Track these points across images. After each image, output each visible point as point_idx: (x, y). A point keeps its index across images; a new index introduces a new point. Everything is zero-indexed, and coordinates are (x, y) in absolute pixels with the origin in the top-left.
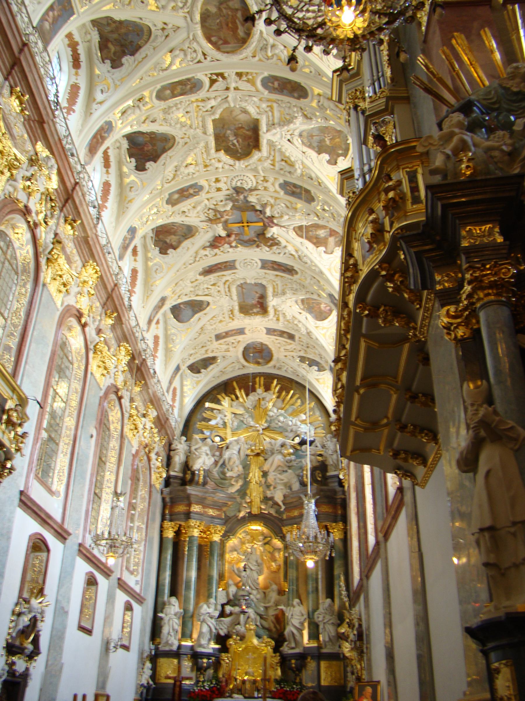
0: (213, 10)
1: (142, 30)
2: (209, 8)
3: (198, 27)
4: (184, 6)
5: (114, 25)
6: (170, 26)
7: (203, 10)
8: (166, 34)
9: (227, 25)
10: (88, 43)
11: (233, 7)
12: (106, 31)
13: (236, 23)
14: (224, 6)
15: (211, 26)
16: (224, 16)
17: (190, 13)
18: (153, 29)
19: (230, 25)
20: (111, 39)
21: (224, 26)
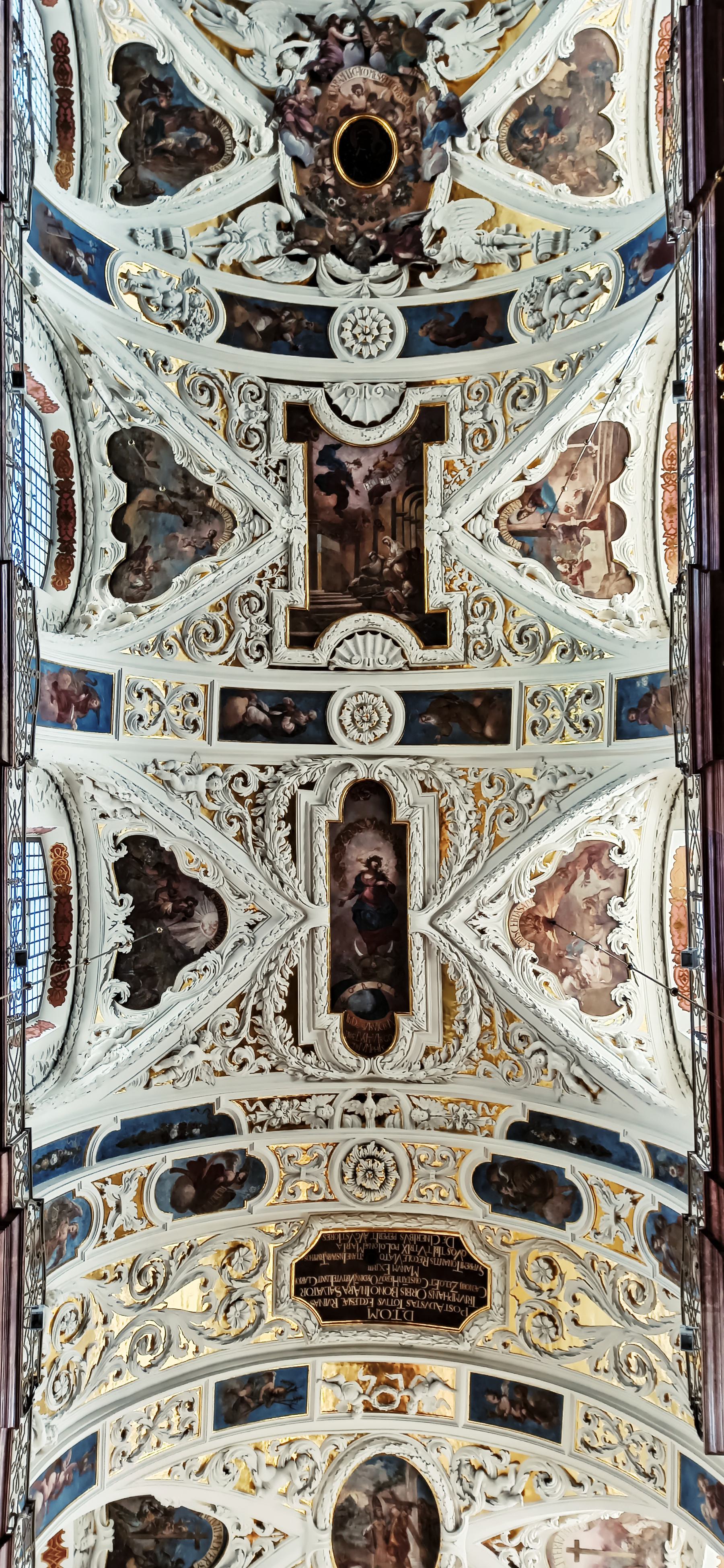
0: (362, 1501)
1: (208, 1535)
2: (354, 1497)
3: (327, 1536)
4: (304, 1488)
5: (152, 1518)
6: (269, 1531)
7: (343, 1500)
8: (257, 1549)
9: (387, 1539)
10: (85, 1557)
11: (403, 1499)
12: (131, 1530)
13: (406, 1537)
14: (385, 1493)
15: (351, 1537)
16: (383, 1517)
17: (316, 1506)
18: (232, 1532)
19: (393, 1540)
20: (135, 1551)
21: (380, 1541)
